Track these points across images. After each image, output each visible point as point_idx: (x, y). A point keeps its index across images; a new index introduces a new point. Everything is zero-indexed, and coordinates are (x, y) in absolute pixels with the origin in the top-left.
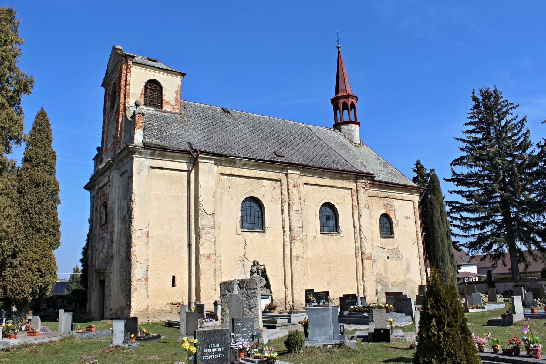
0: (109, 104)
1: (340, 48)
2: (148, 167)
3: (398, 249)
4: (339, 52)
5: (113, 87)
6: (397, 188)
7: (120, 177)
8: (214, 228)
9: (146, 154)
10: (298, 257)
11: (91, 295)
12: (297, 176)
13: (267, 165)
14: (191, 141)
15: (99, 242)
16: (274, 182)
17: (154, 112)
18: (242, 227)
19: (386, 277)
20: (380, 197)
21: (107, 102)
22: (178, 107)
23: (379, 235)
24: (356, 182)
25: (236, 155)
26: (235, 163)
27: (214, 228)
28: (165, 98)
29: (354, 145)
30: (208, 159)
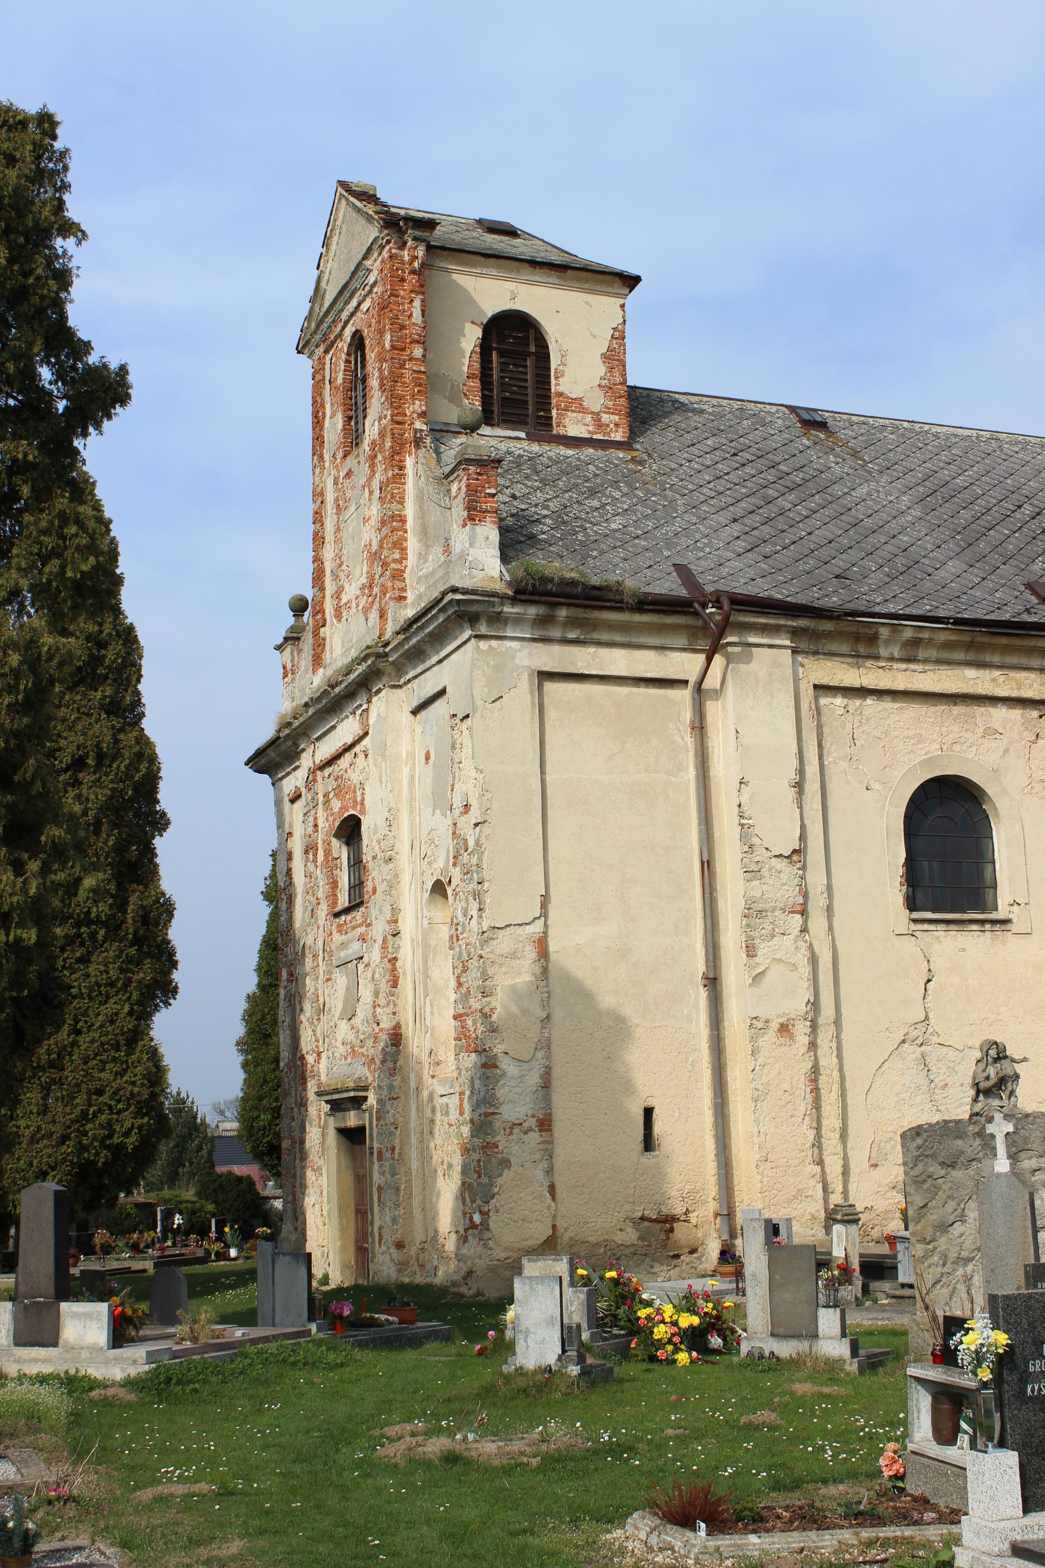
0: (334, 425)
2: (530, 675)
5: (348, 354)
7: (412, 717)
11: (297, 1189)
14: (688, 559)
15: (328, 980)
17: (525, 444)
18: (912, 904)
21: (328, 413)
22: (616, 418)
25: (877, 609)
30: (764, 629)
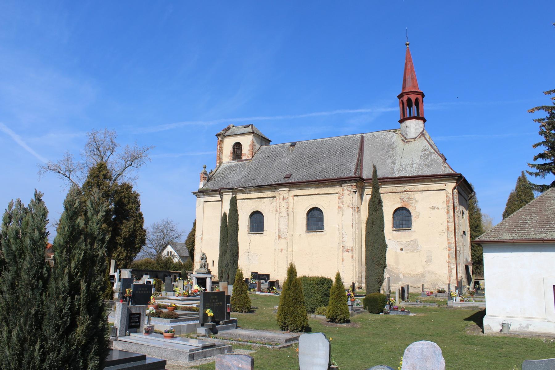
1: (408, 45)
3: (415, 241)
4: (408, 49)
6: (416, 181)
10: (282, 250)
12: (286, 192)
13: (262, 188)
16: (272, 199)
19: (396, 268)
23: (391, 229)
24: (342, 187)
26: (244, 191)
28: (243, 152)
29: (406, 141)
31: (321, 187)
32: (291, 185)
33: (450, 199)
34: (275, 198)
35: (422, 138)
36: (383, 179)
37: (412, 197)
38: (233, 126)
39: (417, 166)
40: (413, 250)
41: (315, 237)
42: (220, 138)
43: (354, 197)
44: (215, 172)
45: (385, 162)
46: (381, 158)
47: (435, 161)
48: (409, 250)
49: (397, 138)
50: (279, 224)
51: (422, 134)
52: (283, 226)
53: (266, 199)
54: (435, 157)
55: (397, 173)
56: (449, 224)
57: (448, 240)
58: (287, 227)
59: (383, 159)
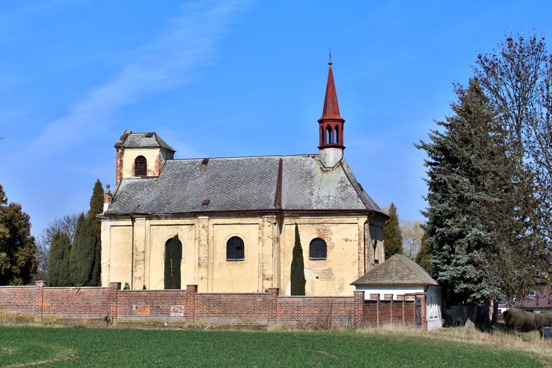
3: (330, 270)
6: (331, 214)
8: (144, 261)
9: (108, 219)
10: (202, 278)
16: (190, 226)
20: (313, 224)
22: (157, 172)
24: (262, 218)
27: (144, 261)
28: (148, 168)
29: (324, 169)
31: (242, 217)
32: (212, 214)
33: (361, 232)
34: (194, 226)
35: (340, 168)
36: (301, 210)
37: (328, 229)
38: (131, 133)
39: (334, 199)
40: (327, 278)
41: (236, 266)
42: (120, 151)
43: (274, 228)
44: (117, 190)
45: (303, 192)
46: (299, 187)
47: (350, 195)
48: (324, 278)
49: (316, 165)
50: (199, 252)
51: (341, 163)
52: (203, 255)
53: (184, 226)
54: (350, 191)
55: (314, 205)
56: (361, 255)
57: (359, 269)
58: (207, 256)
59: (301, 189)
